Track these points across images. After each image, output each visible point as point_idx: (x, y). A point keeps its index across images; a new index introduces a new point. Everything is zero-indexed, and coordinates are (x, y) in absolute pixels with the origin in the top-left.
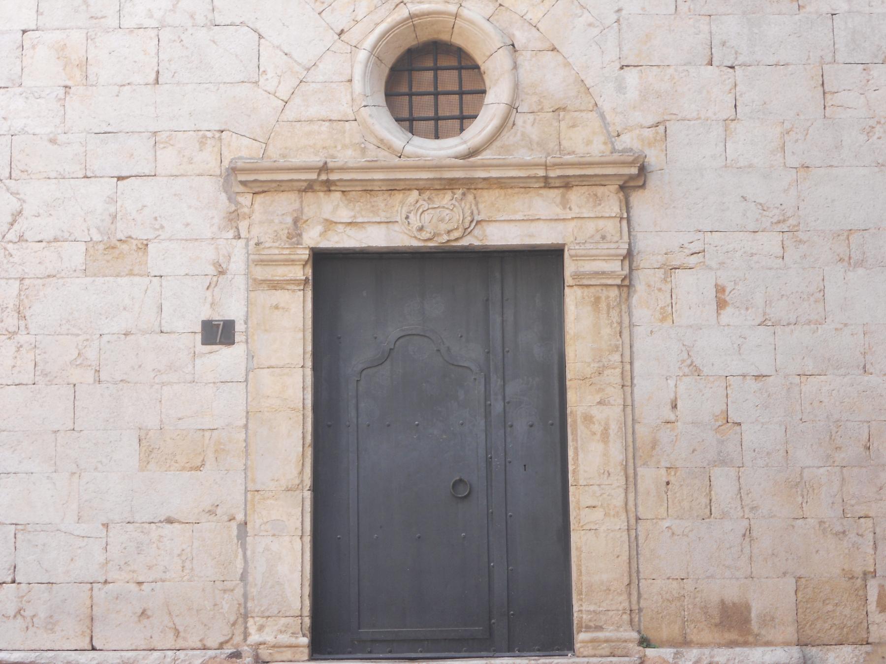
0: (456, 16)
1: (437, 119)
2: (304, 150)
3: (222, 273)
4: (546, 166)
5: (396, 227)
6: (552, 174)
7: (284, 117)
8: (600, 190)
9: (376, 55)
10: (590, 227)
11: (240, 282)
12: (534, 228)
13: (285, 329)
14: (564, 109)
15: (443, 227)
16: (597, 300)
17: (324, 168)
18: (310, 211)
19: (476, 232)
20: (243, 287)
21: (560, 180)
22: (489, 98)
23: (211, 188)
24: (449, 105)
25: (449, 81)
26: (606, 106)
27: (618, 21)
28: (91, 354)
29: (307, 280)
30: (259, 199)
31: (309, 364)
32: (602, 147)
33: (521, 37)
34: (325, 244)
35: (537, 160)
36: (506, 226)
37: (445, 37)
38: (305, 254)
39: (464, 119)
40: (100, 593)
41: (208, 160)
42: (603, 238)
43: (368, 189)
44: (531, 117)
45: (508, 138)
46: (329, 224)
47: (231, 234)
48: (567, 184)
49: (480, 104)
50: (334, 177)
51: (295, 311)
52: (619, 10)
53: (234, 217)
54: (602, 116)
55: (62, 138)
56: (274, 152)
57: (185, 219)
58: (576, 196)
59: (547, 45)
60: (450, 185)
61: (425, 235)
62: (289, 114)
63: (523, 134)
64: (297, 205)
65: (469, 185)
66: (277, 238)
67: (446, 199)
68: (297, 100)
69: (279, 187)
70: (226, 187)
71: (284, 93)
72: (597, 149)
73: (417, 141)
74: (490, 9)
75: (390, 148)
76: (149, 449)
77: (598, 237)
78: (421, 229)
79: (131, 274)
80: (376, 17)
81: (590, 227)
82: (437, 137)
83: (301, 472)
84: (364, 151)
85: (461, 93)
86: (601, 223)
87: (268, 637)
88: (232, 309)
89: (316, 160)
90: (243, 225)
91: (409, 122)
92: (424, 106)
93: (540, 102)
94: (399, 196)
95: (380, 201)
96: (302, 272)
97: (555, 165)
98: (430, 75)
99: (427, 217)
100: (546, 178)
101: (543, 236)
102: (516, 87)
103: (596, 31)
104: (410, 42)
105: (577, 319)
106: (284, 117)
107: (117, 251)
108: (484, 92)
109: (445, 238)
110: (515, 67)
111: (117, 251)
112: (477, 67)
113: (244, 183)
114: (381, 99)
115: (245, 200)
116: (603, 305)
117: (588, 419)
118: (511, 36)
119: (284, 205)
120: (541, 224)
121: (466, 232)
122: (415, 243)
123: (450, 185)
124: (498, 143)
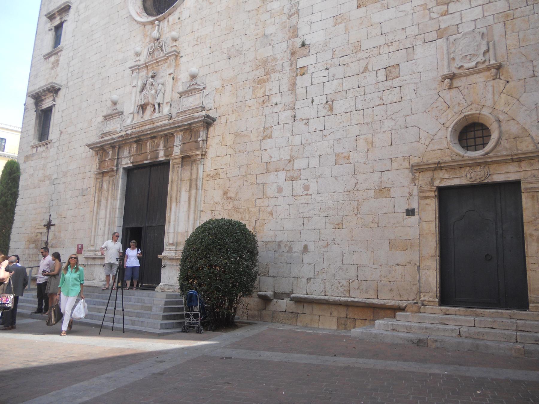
0: (479, 114)
1: (475, 145)
2: (433, 158)
3: (411, 195)
4: (512, 155)
5: (463, 178)
6: (514, 158)
7: (427, 150)
8: (532, 161)
9: (454, 129)
10: (529, 173)
11: (416, 198)
12: (509, 175)
13: (430, 211)
14: (518, 137)
15: (478, 177)
16: (533, 196)
17: (439, 163)
18: (436, 176)
19: (489, 178)
20: (417, 199)
21: (518, 159)
22: (492, 137)
23: (407, 172)
24: (479, 141)
25: (479, 134)
26: (533, 134)
27: (536, 107)
28: (376, 219)
29: (436, 196)
30: (421, 174)
31: (437, 220)
32: (533, 148)
33: (501, 117)
34: (441, 185)
35: (508, 154)
36: (499, 175)
37: (477, 121)
38: (434, 188)
39: (484, 145)
40: (379, 284)
41: (406, 164)
42: (534, 176)
43: (453, 168)
44: (506, 141)
45: (499, 148)
46: (442, 179)
47: (413, 184)
48: (520, 160)
49: (490, 139)
50: (442, 165)
52: (536, 104)
53: (414, 180)
54: (532, 138)
55: (367, 162)
56: (425, 160)
57: (401, 181)
58: (523, 164)
59: (511, 118)
60: (480, 164)
61: (472, 180)
62: (429, 149)
63: (504, 146)
64: (432, 175)
65: (486, 164)
66: (426, 184)
67: (478, 169)
68: (431, 145)
69: (427, 170)
70: (411, 171)
71: (427, 143)
72: (531, 148)
73: (469, 152)
74: (491, 110)
75: (460, 155)
76: (392, 245)
77: (532, 176)
78: (471, 178)
79: (386, 197)
80: (454, 118)
81: (529, 173)
82: (476, 151)
83: (436, 252)
84: (452, 157)
85: (483, 137)
86: (533, 172)
87: (427, 298)
88: (415, 206)
89: (436, 161)
90: (417, 182)
91: (466, 147)
92: (471, 142)
93: (509, 136)
94: (464, 169)
95: (457, 171)
97: (514, 155)
98: (473, 133)
99: (472, 175)
100: (512, 159)
101: (513, 177)
102: (500, 132)
103: (528, 112)
104: (466, 124)
105: (526, 203)
106: (427, 150)
107: (382, 191)
108: (490, 136)
109: (479, 180)
110: (500, 126)
112: (488, 128)
113: (416, 170)
114: (457, 141)
115: (417, 174)
116: (535, 198)
117: (531, 235)
118: (498, 118)
119: (428, 175)
120: (512, 174)
121: (486, 178)
122: (469, 183)
123: (480, 164)
124: (495, 150)
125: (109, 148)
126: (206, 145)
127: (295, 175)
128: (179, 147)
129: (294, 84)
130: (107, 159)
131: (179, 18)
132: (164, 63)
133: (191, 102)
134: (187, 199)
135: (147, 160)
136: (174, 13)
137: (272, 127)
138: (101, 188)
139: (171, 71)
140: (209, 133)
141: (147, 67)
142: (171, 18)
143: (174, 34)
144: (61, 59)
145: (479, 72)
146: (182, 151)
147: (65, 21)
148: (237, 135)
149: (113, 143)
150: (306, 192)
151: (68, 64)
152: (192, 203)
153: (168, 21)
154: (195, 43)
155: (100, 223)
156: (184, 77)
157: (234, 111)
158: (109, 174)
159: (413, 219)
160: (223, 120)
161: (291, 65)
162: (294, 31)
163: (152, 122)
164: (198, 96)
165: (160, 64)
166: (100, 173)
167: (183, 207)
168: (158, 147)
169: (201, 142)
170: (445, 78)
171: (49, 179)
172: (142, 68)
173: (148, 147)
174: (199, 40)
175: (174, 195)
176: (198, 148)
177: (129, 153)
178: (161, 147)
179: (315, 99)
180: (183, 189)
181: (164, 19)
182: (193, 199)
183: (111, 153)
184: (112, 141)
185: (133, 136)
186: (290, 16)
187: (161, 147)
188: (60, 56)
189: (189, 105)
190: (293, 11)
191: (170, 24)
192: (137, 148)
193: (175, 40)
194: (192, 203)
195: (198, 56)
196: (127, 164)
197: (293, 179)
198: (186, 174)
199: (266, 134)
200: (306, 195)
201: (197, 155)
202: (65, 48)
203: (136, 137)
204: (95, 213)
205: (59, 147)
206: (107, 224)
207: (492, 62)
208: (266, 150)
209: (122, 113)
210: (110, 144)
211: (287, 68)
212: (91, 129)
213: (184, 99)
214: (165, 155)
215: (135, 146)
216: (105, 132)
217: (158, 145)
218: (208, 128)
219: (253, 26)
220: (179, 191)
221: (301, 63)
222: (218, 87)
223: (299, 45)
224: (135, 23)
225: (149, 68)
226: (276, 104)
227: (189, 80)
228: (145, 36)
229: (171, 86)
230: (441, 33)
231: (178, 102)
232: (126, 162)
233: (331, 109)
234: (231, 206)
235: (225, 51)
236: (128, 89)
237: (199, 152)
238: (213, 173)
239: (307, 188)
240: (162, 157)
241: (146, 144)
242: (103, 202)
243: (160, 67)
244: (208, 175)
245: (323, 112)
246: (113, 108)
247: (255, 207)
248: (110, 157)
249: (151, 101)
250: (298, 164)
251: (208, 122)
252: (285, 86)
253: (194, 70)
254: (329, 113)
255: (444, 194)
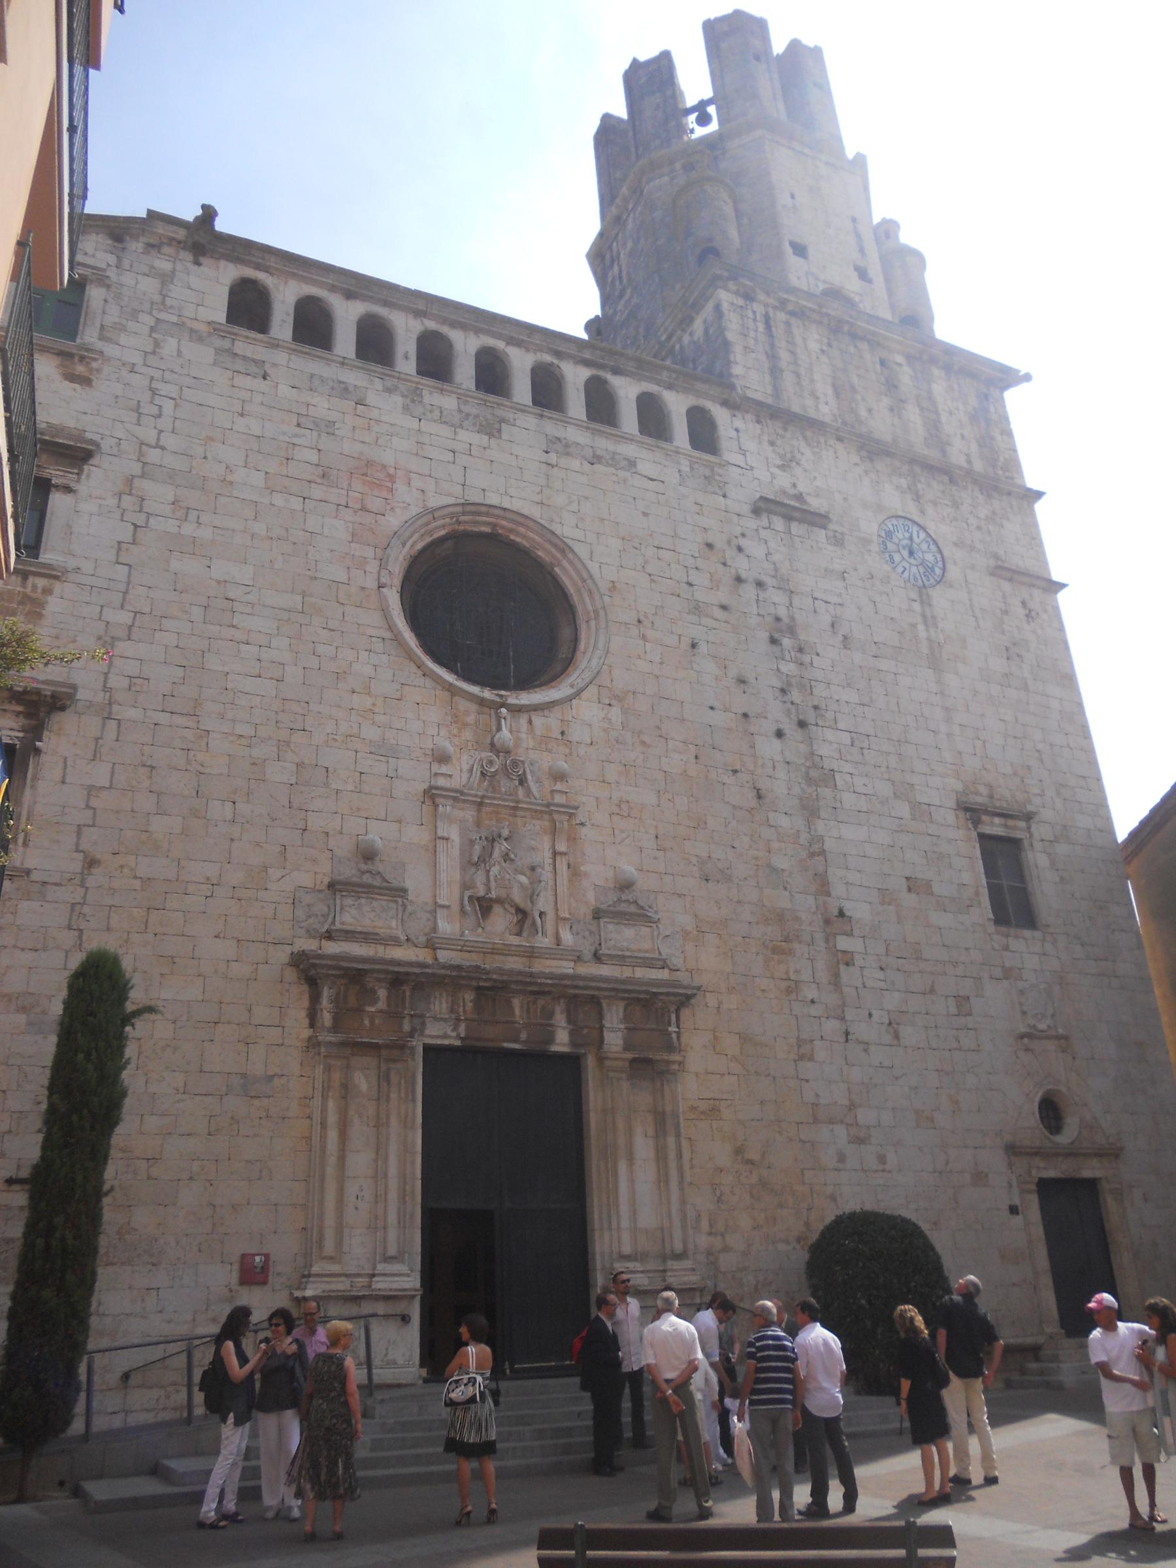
21: (1100, 1154)
48: (1101, 1155)
51: (1033, 1201)
53: (1010, 1165)
88: (1017, 1201)
96: (1034, 1187)
107: (980, 1178)
111: (980, 1178)
125: (379, 980)
126: (680, 1044)
127: (862, 1135)
128: (620, 1034)
129: (837, 975)
130: (373, 1009)
131: (563, 733)
132: (532, 818)
133: (624, 937)
134: (652, 1155)
135: (516, 1041)
136: (546, 712)
137: (812, 1041)
138: (346, 1090)
139: (561, 847)
140: (682, 1018)
141: (481, 804)
142: (538, 720)
143: (563, 765)
144: (53, 605)
145: (1048, 1038)
146: (627, 1048)
147: (68, 489)
148: (745, 1038)
149: (407, 974)
150: (881, 1167)
151: (108, 642)
152: (673, 1165)
153: (530, 722)
154: (616, 810)
155: (351, 1189)
156: (597, 873)
157: (731, 990)
158: (384, 1052)
159: (1018, 1220)
160: (711, 1000)
161: (827, 941)
162: (823, 886)
163: (531, 954)
164: (645, 931)
165: (519, 813)
166: (343, 1044)
167: (646, 1173)
168: (550, 1018)
169: (674, 1036)
170: (1022, 1036)
171: (23, 1009)
172: (465, 801)
173: (517, 1011)
174: (624, 807)
175: (621, 1141)
176: (670, 1048)
177: (452, 1011)
178: (560, 1019)
179: (874, 1012)
180: (639, 1131)
181: (519, 711)
182: (672, 1155)
183: (382, 993)
184: (417, 970)
185: (495, 976)
186: (812, 855)
187: (560, 1019)
188: (48, 591)
189: (625, 944)
190: (816, 848)
191: (538, 732)
192: (476, 1002)
193: (560, 777)
194: (673, 1165)
195: (627, 841)
196: (445, 1036)
197: (860, 1141)
198: (643, 1098)
199: (803, 1053)
200: (883, 1171)
201: (668, 1062)
202: (72, 577)
203: (495, 981)
204: (332, 1160)
205: (86, 910)
206: (393, 1195)
207: (1060, 1031)
208: (807, 1081)
209: (402, 892)
210: (398, 972)
211: (821, 944)
212: (262, 894)
213: (611, 927)
214: (573, 1043)
215: (469, 996)
216: (338, 926)
217: (551, 1015)
218: (677, 1012)
219: (746, 839)
220: (630, 1131)
221: (843, 943)
222: (689, 928)
223: (836, 912)
224: (413, 668)
225: (485, 809)
226: (813, 1001)
227: (612, 886)
228: (457, 719)
229: (565, 882)
230: (1008, 973)
231: (594, 928)
232: (441, 1030)
233: (897, 1036)
234: (754, 1179)
235: (694, 860)
236: (416, 835)
237: (676, 1057)
238: (703, 1106)
239: (882, 1159)
240: (564, 1045)
241: (509, 1003)
242: (359, 1130)
243: (519, 821)
244: (693, 1108)
245: (887, 1039)
246: (364, 867)
247: (804, 1183)
248: (382, 1005)
249: (517, 896)
250: (865, 1116)
251: (684, 999)
252: (823, 976)
253: (629, 869)
254: (895, 1042)
255: (1046, 1188)
